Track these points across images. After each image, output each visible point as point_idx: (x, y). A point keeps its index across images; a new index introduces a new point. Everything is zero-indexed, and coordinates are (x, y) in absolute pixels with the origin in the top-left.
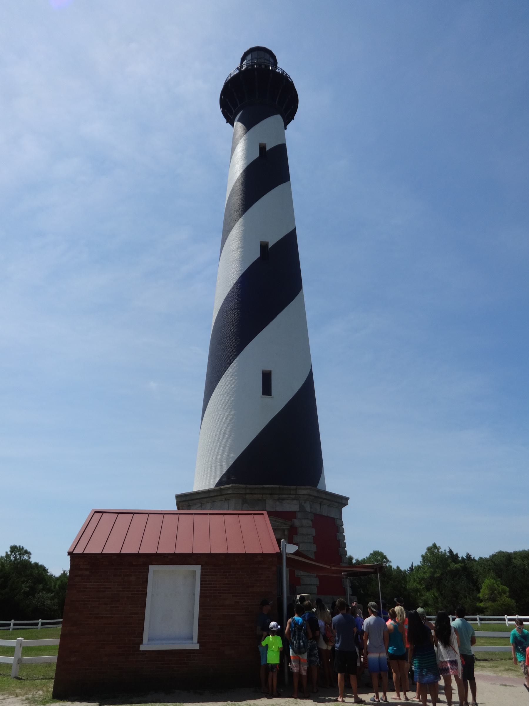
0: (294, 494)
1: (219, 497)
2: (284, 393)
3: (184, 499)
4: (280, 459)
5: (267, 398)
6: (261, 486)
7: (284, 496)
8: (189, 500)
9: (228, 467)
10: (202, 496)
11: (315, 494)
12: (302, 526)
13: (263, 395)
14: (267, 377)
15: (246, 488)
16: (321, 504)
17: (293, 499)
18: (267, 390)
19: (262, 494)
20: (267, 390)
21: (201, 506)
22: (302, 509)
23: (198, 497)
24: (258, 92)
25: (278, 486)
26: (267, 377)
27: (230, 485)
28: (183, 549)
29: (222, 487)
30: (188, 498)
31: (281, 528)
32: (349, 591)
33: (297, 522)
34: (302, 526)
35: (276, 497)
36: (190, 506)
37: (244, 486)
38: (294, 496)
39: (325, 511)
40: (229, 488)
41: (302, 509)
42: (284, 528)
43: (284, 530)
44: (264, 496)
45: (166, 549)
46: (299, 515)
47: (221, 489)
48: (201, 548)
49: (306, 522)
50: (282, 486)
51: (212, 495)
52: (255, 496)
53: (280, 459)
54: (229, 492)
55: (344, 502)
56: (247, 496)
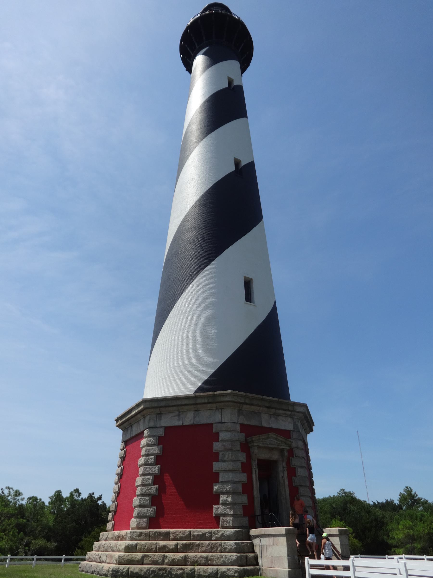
0: (291, 411)
1: (209, 405)
3: (155, 405)
5: (249, 306)
6: (261, 397)
7: (281, 412)
8: (160, 407)
9: (211, 373)
10: (188, 402)
12: (298, 448)
13: (246, 301)
14: (248, 284)
15: (245, 397)
17: (288, 416)
18: (249, 298)
19: (260, 406)
20: (249, 298)
21: (179, 415)
23: (179, 403)
24: (217, 36)
25: (277, 399)
26: (248, 284)
27: (229, 391)
29: (217, 393)
30: (162, 404)
31: (282, 447)
34: (298, 448)
35: (273, 411)
36: (161, 414)
37: (244, 394)
38: (289, 413)
40: (227, 395)
42: (284, 447)
43: (282, 451)
44: (261, 408)
47: (214, 396)
50: (281, 400)
51: (199, 401)
52: (253, 407)
56: (245, 407)
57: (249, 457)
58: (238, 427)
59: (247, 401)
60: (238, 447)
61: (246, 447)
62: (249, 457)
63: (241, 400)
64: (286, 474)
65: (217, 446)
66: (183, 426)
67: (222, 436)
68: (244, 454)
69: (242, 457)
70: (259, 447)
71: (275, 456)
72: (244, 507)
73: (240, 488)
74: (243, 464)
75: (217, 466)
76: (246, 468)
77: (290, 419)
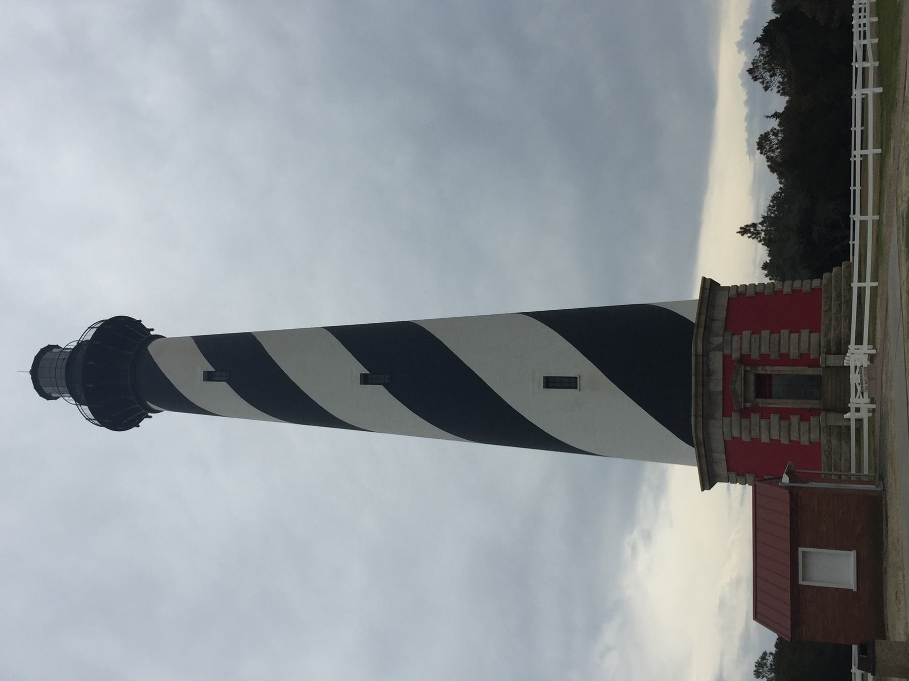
2: (569, 359)
3: (707, 484)
4: (657, 365)
5: (582, 383)
11: (701, 330)
12: (741, 349)
14: (550, 383)
16: (712, 320)
18: (570, 383)
20: (570, 383)
22: (720, 348)
26: (550, 383)
28: (787, 559)
30: (706, 478)
32: (816, 283)
33: (736, 355)
39: (721, 313)
41: (720, 348)
43: (746, 371)
45: (787, 572)
46: (727, 352)
47: (697, 443)
48: (787, 546)
49: (736, 345)
53: (657, 365)
54: (701, 436)
55: (708, 286)
57: (755, 409)
58: (727, 420)
59: (701, 413)
60: (745, 422)
61: (745, 413)
62: (755, 409)
63: (700, 419)
64: (768, 368)
65: (745, 438)
66: (727, 461)
67: (736, 434)
68: (753, 415)
69: (755, 417)
70: (746, 401)
71: (752, 378)
72: (801, 420)
73: (784, 423)
74: (761, 417)
75: (764, 439)
76: (765, 414)
77: (711, 355)
